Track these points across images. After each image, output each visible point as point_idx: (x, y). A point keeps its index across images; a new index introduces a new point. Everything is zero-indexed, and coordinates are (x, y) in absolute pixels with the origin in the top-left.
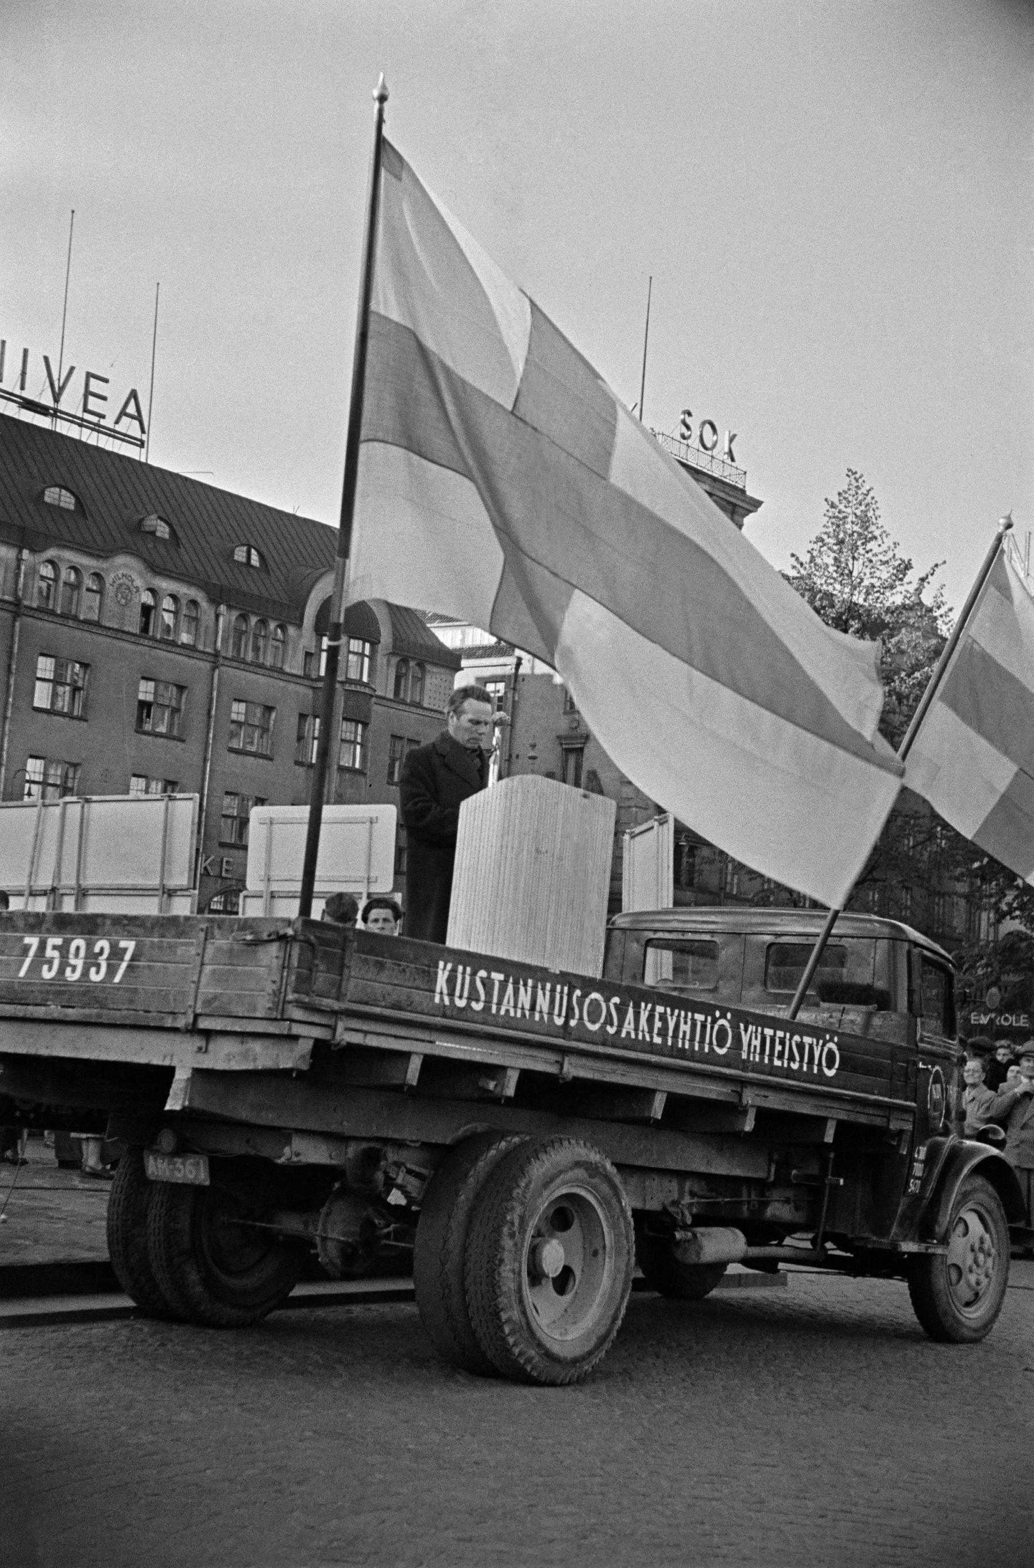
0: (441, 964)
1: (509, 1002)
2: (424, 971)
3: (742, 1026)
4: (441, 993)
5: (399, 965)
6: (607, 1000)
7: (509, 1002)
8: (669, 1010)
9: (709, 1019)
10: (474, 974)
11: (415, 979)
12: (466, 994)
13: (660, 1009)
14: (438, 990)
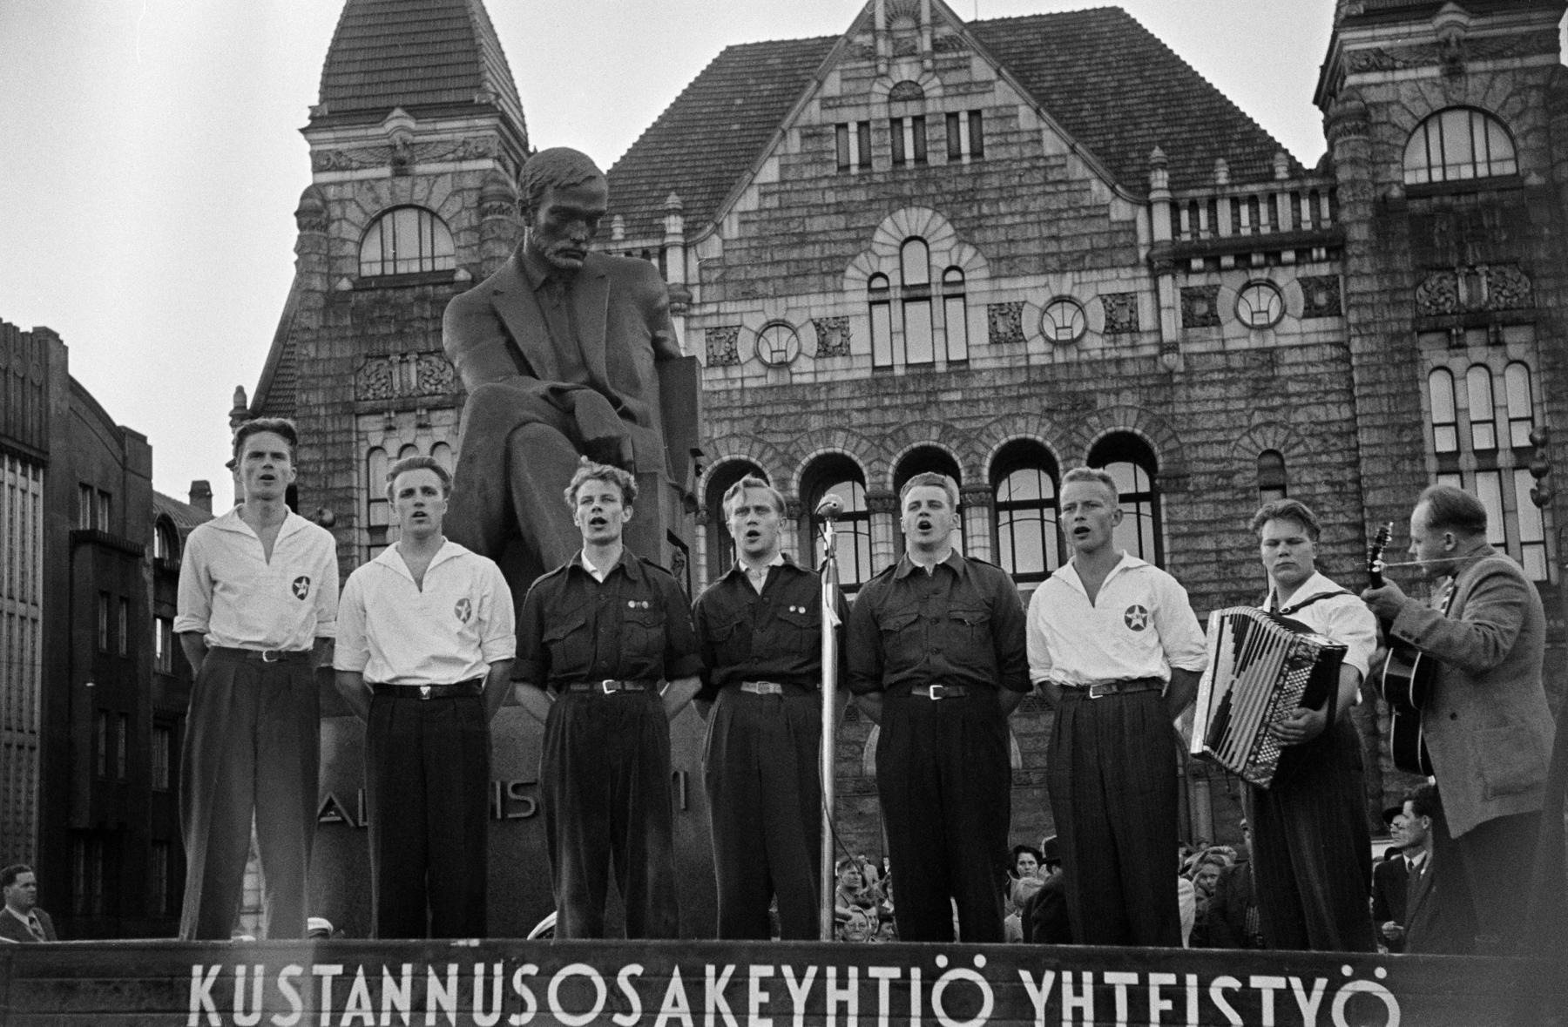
0: (197, 970)
1: (359, 1005)
2: (158, 985)
3: (1025, 975)
4: (203, 1011)
5: (108, 983)
6: (610, 975)
7: (359, 1005)
8: (787, 970)
9: (916, 973)
10: (272, 974)
11: (142, 999)
12: (257, 1004)
13: (758, 972)
14: (194, 1005)
